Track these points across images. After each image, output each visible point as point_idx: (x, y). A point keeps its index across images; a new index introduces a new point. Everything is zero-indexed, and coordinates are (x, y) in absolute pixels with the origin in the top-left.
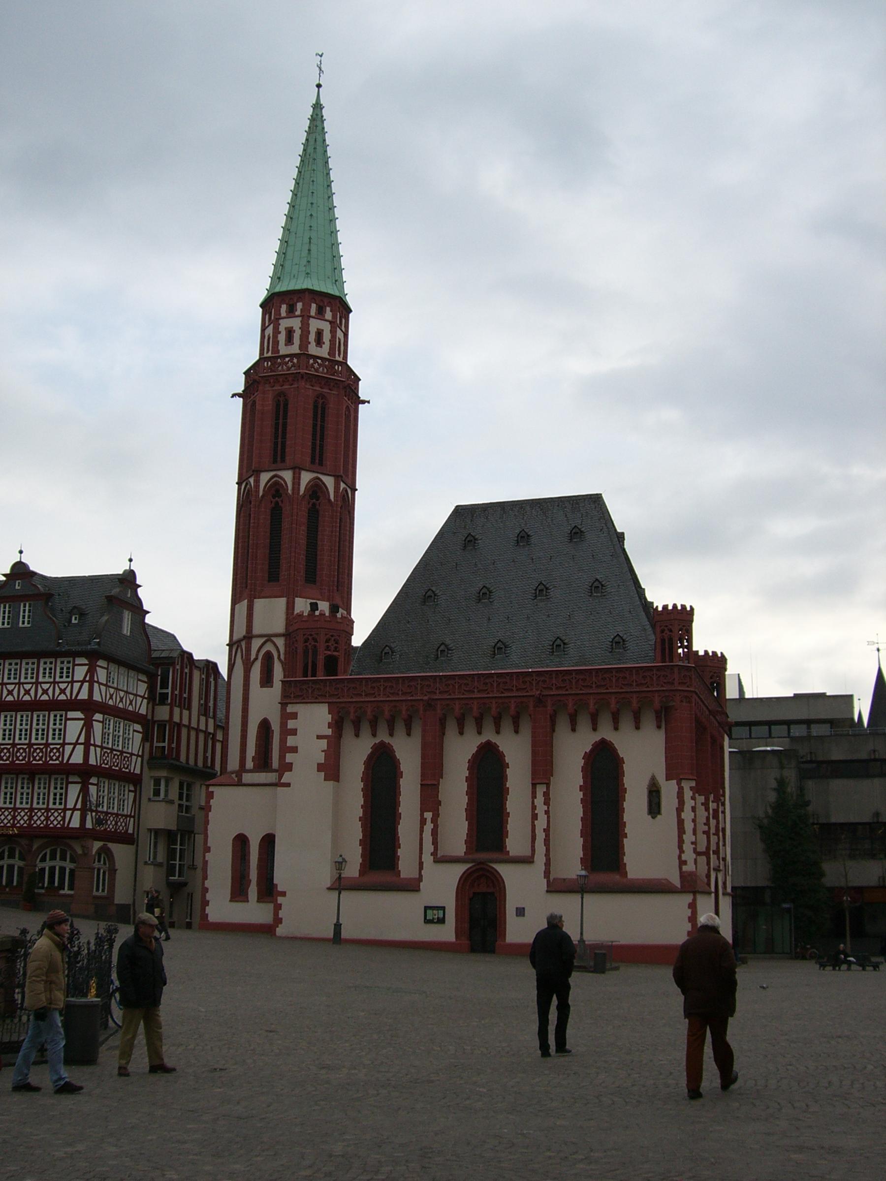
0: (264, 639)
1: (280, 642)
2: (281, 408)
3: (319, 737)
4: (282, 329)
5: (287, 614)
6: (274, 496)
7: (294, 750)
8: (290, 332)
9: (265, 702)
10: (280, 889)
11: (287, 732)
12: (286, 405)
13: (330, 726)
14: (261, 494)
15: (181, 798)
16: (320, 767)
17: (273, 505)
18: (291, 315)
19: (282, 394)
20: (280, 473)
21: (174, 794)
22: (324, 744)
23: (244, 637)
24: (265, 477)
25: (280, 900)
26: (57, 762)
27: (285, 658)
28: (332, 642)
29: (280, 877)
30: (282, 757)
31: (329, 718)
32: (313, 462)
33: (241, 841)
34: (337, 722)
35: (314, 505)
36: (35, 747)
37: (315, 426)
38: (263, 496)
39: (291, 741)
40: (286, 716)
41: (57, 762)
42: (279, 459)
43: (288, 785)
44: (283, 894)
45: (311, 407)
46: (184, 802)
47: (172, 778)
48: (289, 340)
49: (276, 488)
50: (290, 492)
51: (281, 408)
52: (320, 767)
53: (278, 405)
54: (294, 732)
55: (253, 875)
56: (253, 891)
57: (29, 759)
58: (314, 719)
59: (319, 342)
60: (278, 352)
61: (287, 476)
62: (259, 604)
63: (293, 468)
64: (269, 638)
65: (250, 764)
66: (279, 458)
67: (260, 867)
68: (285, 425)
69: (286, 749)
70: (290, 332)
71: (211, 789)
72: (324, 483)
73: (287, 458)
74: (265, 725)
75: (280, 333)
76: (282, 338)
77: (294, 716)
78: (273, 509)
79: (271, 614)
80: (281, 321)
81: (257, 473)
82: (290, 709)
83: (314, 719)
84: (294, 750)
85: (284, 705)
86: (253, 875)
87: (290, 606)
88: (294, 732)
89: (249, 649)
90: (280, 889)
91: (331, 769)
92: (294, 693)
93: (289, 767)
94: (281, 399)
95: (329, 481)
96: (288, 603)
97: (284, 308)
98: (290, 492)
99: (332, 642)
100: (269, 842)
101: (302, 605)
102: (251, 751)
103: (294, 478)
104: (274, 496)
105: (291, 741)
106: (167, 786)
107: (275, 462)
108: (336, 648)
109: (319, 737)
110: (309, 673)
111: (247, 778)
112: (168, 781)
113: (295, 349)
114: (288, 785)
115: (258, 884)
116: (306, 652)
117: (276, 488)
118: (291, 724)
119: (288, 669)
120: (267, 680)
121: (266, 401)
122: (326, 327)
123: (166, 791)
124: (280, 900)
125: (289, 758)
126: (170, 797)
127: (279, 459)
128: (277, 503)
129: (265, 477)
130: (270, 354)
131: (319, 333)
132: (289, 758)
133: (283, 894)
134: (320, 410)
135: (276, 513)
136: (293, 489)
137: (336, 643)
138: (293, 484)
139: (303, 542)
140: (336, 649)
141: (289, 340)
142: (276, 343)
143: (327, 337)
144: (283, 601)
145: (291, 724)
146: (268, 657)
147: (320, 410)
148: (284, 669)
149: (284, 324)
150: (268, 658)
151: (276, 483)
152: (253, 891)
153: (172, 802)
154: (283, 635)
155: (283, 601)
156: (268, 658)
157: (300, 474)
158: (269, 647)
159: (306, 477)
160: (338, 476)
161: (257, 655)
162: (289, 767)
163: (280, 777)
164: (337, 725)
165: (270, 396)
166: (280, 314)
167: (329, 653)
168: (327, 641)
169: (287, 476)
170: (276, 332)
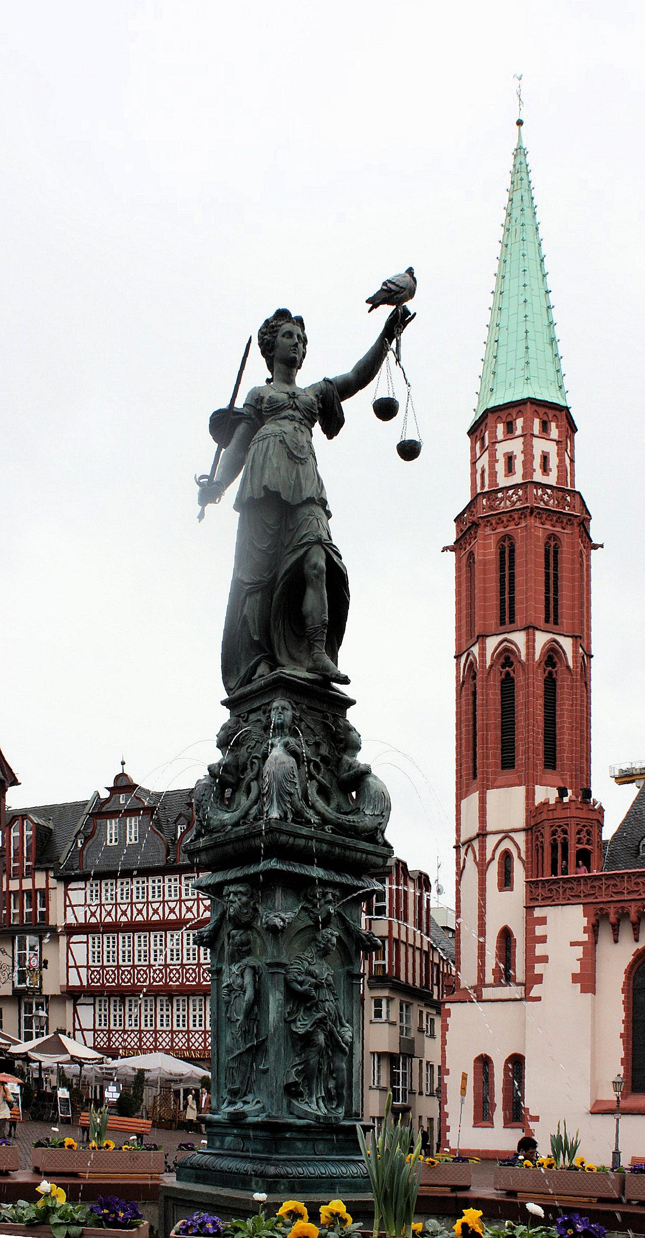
0: (500, 836)
1: (520, 838)
2: (507, 554)
3: (573, 944)
4: (500, 456)
5: (527, 805)
6: (503, 666)
7: (544, 959)
8: (510, 459)
9: (507, 908)
10: (532, 1113)
11: (533, 940)
12: (512, 551)
13: (585, 930)
14: (488, 663)
15: (401, 1021)
16: (575, 978)
17: (503, 676)
18: (510, 436)
19: (507, 537)
20: (512, 636)
21: (395, 1017)
22: (579, 951)
23: (478, 835)
24: (492, 643)
25: (532, 1125)
26: (194, 983)
27: (527, 857)
28: (584, 834)
29: (531, 1102)
30: (529, 968)
31: (584, 922)
32: (547, 620)
33: (484, 1062)
34: (593, 926)
35: (550, 673)
36: (187, 967)
37: (547, 575)
38: (491, 666)
39: (540, 949)
40: (531, 922)
41: (194, 983)
42: (507, 620)
43: (538, 999)
44: (536, 1119)
45: (542, 551)
46: (404, 1024)
47: (392, 999)
48: (510, 469)
49: (507, 656)
50: (523, 658)
51: (507, 554)
52: (575, 978)
53: (502, 553)
54: (543, 939)
55: (499, 1098)
56: (498, 1115)
57: (166, 980)
58: (567, 923)
59: (545, 469)
60: (497, 485)
61: (519, 638)
62: (491, 794)
63: (526, 629)
64: (507, 834)
65: (489, 978)
66: (507, 616)
67: (505, 1090)
68: (512, 576)
69: (532, 959)
70: (510, 459)
71: (447, 1006)
72: (561, 647)
73: (517, 617)
74: (506, 935)
75: (497, 461)
76: (500, 467)
77: (543, 921)
78: (503, 682)
79: (508, 806)
80: (498, 446)
81: (483, 637)
82: (538, 913)
83: (567, 923)
84: (544, 959)
85: (529, 909)
86: (499, 1098)
87: (530, 795)
88: (543, 939)
89: (483, 848)
90: (532, 1113)
91: (587, 980)
92: (542, 893)
93: (539, 979)
94: (506, 544)
95: (566, 644)
96: (527, 791)
97: (501, 428)
98: (523, 658)
99: (584, 834)
100: (516, 1062)
101: (546, 794)
102: (491, 961)
103: (527, 642)
104: (503, 666)
105: (540, 949)
106: (388, 1006)
107: (502, 623)
108: (588, 840)
109: (573, 944)
110: (559, 871)
111: (487, 993)
112: (389, 1000)
113: (517, 478)
114: (538, 999)
115: (504, 1109)
116: (554, 847)
117: (507, 656)
118: (539, 931)
119: (533, 865)
120: (506, 882)
121: (486, 547)
122: (552, 448)
123: (388, 1012)
124: (532, 1125)
125: (538, 968)
126: (392, 1019)
127: (507, 620)
128: (508, 674)
129: (492, 643)
130: (486, 489)
131: (545, 458)
132: (538, 968)
133: (536, 1119)
134: (552, 556)
135: (508, 686)
136: (528, 654)
137: (589, 835)
138: (528, 648)
139: (540, 718)
140: (588, 842)
141: (510, 469)
142: (493, 474)
143: (553, 462)
144: (521, 791)
145: (539, 931)
146: (507, 855)
147: (552, 556)
148: (526, 869)
149: (502, 449)
150: (507, 855)
151: (506, 650)
152: (498, 1115)
153: (393, 1024)
154: (524, 830)
155: (521, 791)
156: (507, 856)
157: (534, 635)
158: (507, 845)
159: (542, 639)
160: (576, 637)
161: (493, 855)
162: (539, 979)
163: (527, 991)
164: (593, 930)
165: (492, 541)
166: (496, 438)
167: (580, 846)
168: (578, 833)
169: (519, 638)
170: (493, 460)
